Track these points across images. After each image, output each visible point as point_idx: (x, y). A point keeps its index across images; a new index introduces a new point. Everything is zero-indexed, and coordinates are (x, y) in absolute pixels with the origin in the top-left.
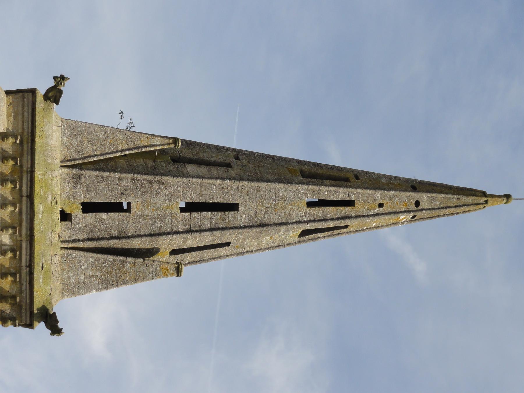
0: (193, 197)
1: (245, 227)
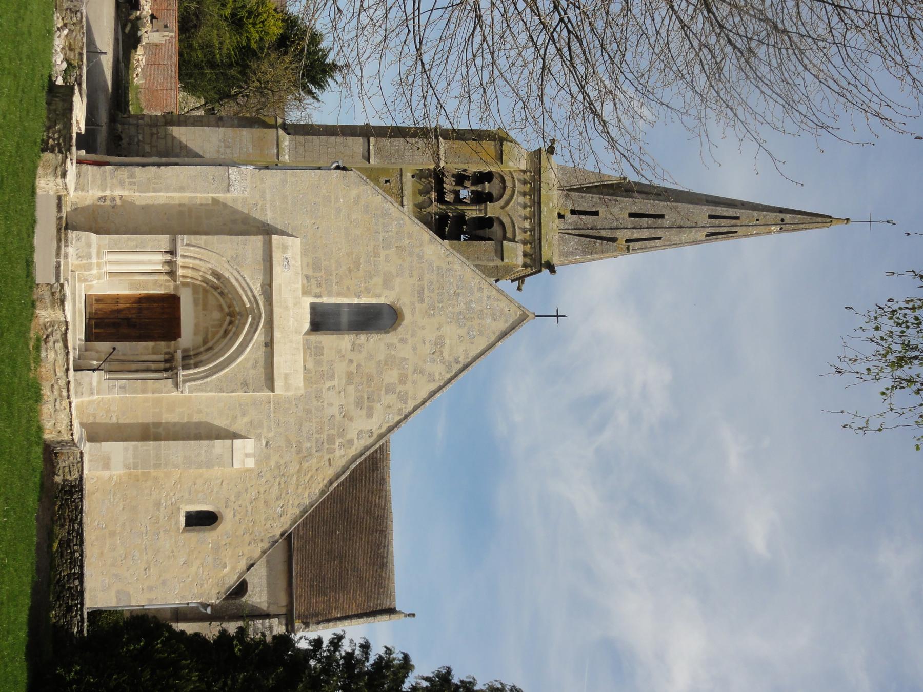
0: (635, 209)
1: (669, 228)
